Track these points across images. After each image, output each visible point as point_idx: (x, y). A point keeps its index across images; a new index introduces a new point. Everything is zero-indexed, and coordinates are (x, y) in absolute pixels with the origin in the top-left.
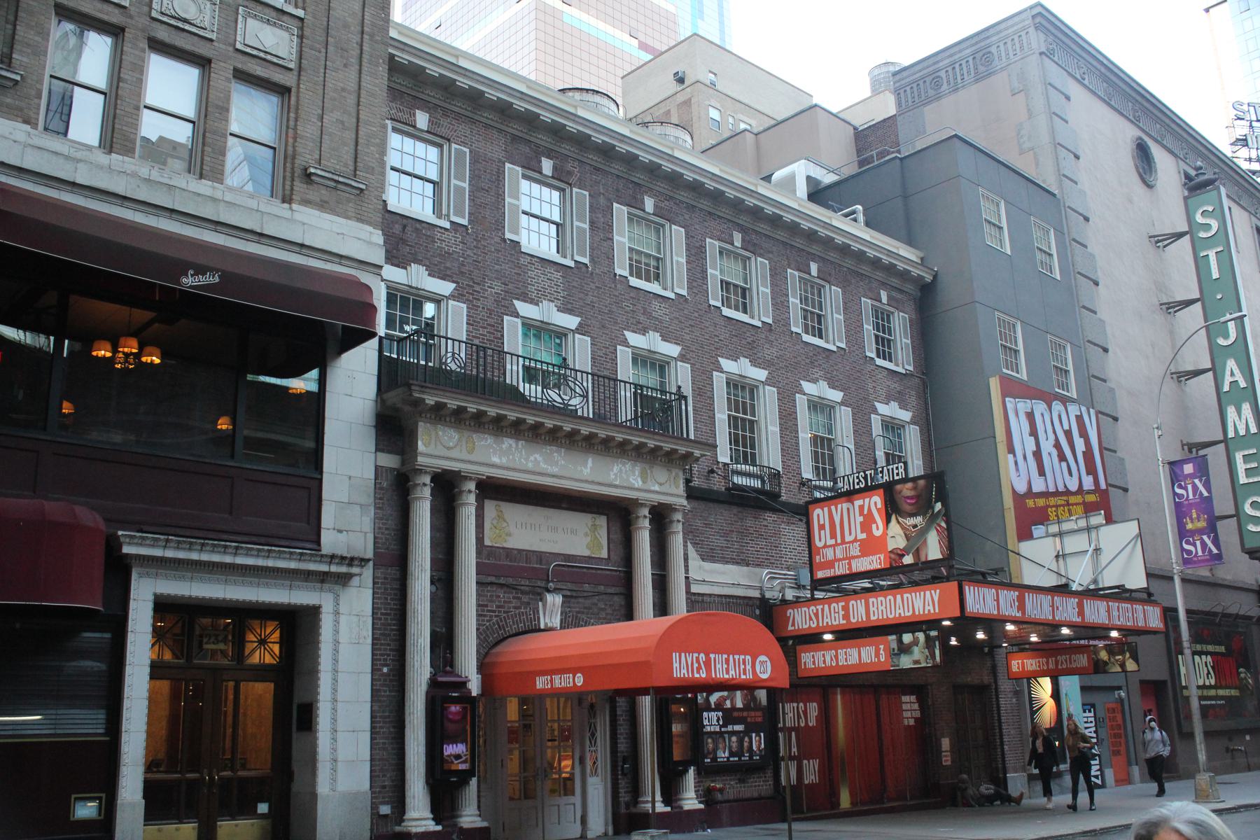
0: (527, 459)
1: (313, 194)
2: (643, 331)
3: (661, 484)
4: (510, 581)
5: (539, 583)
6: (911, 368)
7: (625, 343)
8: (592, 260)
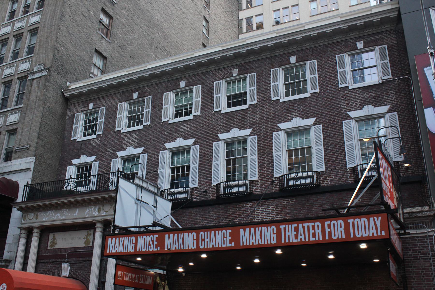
0: (54, 217)
1: (17, 156)
2: (174, 140)
3: (106, 212)
4: (54, 260)
5: (63, 260)
6: (390, 77)
7: (165, 149)
8: (152, 121)
